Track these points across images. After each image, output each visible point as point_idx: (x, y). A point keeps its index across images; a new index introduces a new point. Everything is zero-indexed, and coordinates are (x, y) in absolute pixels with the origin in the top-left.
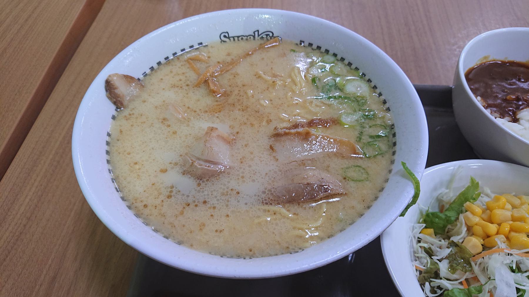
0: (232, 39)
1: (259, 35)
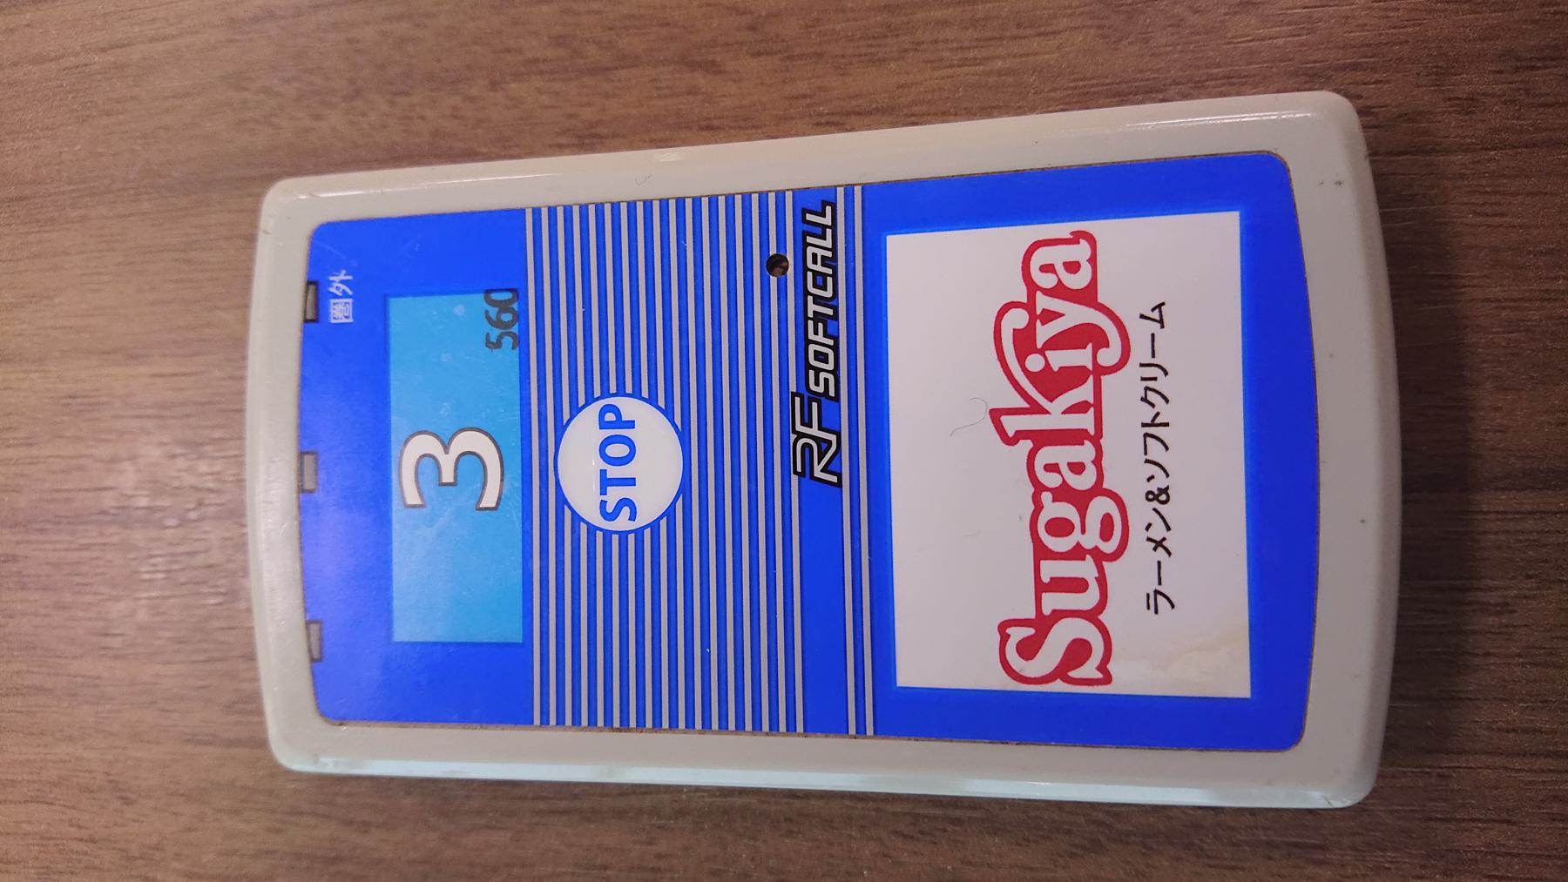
1: (1035, 409)
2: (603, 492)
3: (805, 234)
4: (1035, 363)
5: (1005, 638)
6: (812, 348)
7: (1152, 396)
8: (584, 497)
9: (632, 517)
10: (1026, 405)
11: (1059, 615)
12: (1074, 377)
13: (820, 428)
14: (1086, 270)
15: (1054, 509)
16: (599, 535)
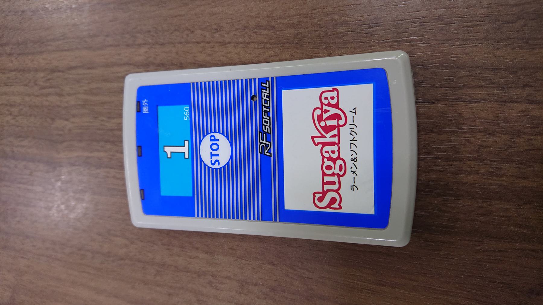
1: (323, 136)
2: (211, 158)
3: (262, 89)
4: (323, 124)
5: (314, 197)
6: (264, 120)
7: (353, 133)
8: (207, 159)
9: (219, 165)
10: (320, 135)
11: (328, 191)
12: (333, 128)
13: (266, 141)
14: (336, 98)
15: (328, 163)
16: (211, 169)
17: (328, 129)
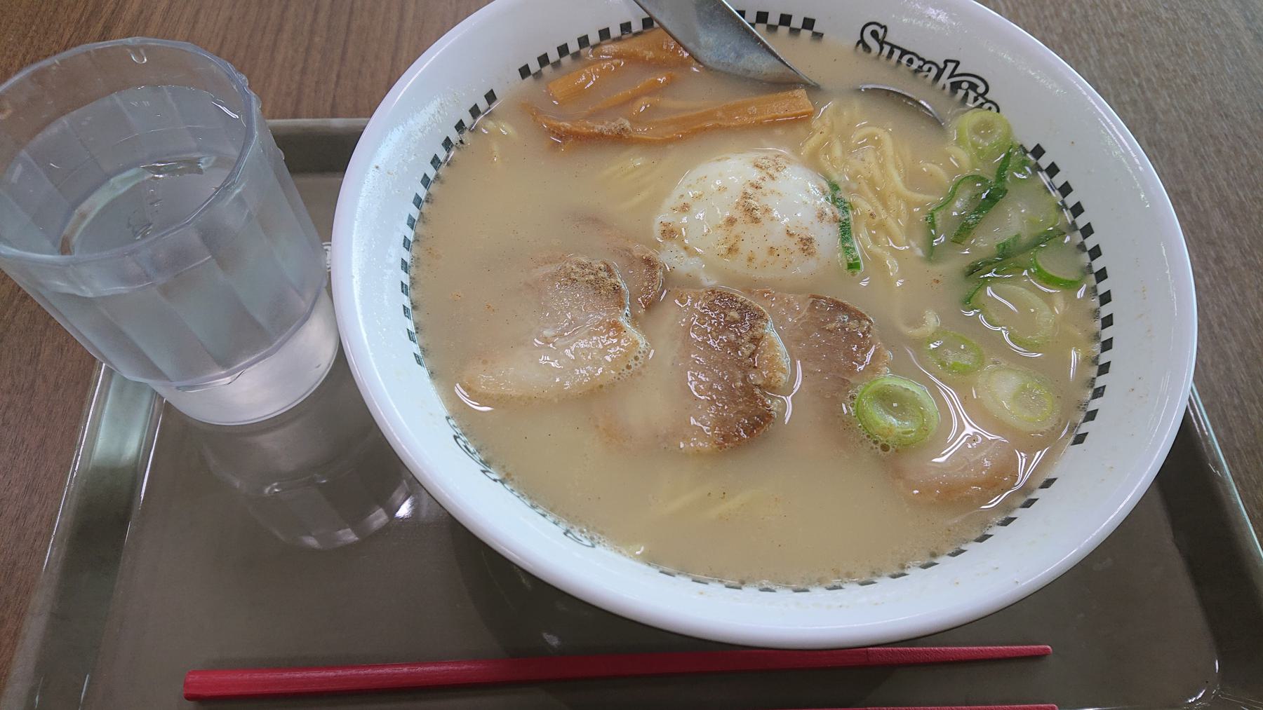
0: (887, 49)
1: (951, 76)
4: (965, 85)
15: (916, 63)
17: (956, 86)
